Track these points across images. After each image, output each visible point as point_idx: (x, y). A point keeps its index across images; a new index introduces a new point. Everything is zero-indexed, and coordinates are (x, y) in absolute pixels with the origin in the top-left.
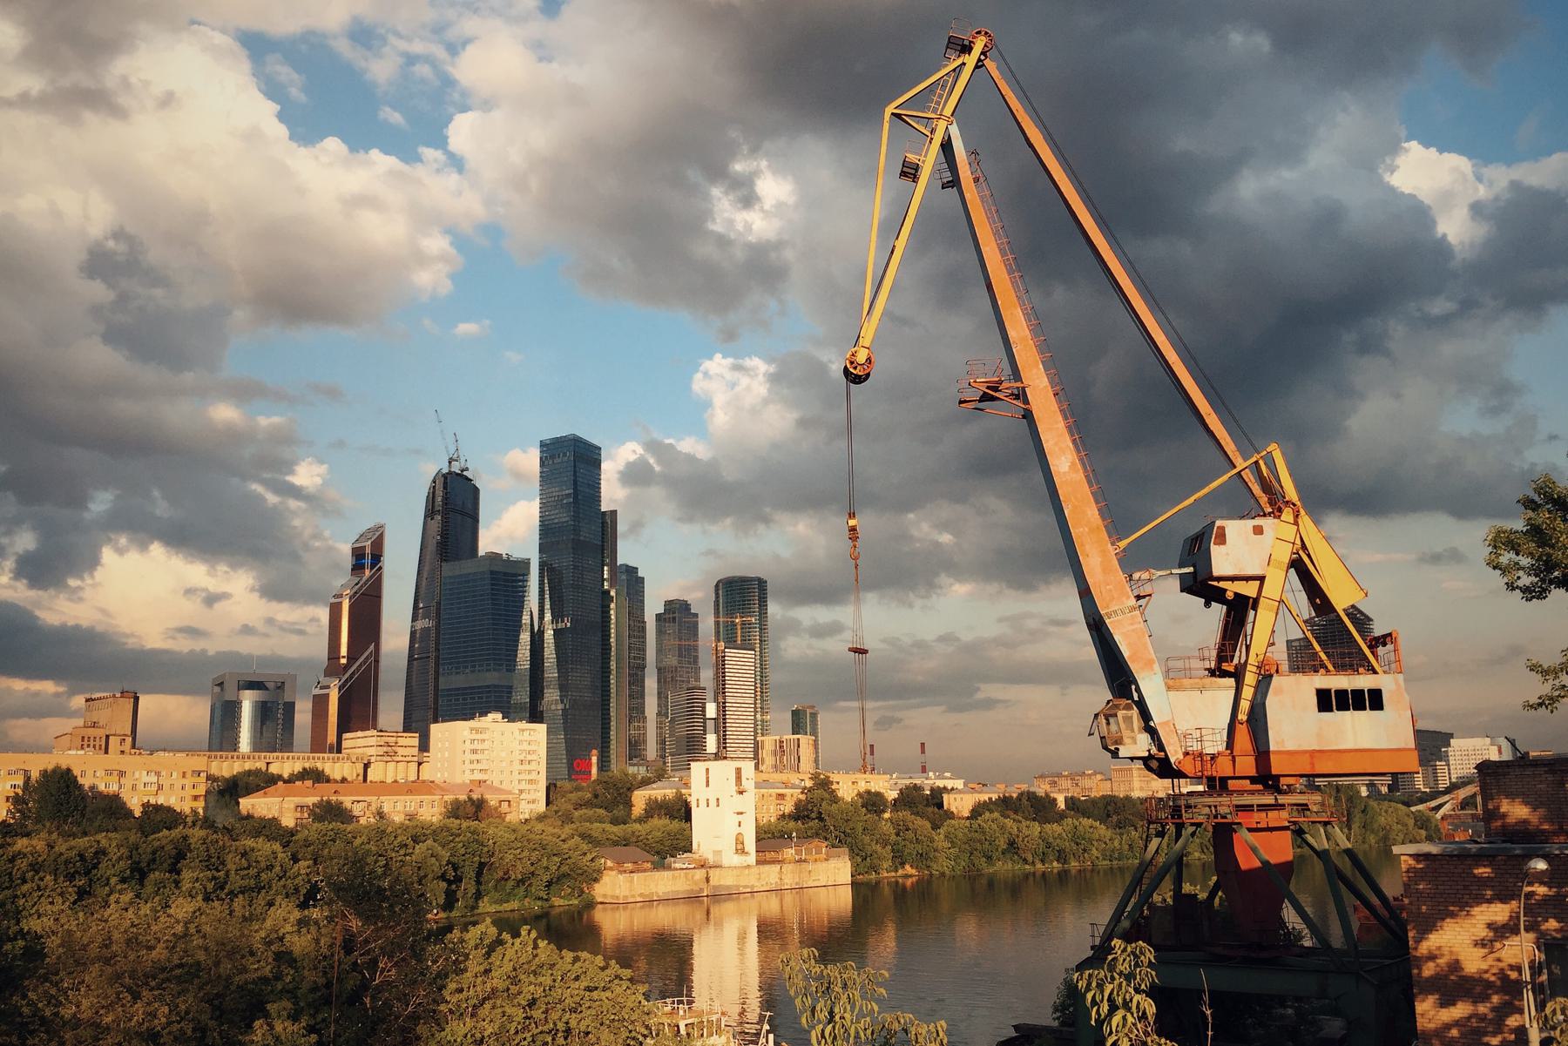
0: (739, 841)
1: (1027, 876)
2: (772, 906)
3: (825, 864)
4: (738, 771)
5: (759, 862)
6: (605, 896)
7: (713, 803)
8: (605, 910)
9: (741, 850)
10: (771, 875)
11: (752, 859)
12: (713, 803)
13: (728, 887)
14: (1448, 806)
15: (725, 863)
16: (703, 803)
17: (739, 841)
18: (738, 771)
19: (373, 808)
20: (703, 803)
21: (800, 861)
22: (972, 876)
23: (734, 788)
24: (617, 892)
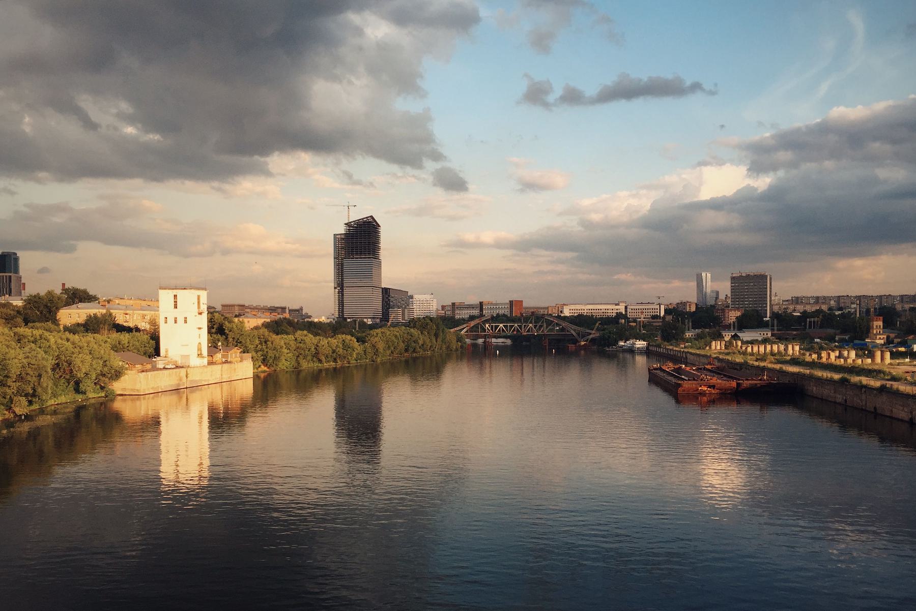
0: (200, 349)
1: (320, 371)
2: (218, 396)
3: (240, 364)
4: (199, 297)
5: (211, 363)
6: (124, 389)
7: (181, 320)
8: (125, 400)
9: (200, 355)
10: (217, 373)
11: (205, 361)
12: (181, 320)
13: (195, 381)
14: (465, 330)
15: (192, 364)
16: (171, 320)
17: (200, 349)
18: (199, 297)
19: (148, 318)
20: (171, 320)
21: (227, 362)
22: (297, 371)
23: (196, 310)
24: (138, 387)
